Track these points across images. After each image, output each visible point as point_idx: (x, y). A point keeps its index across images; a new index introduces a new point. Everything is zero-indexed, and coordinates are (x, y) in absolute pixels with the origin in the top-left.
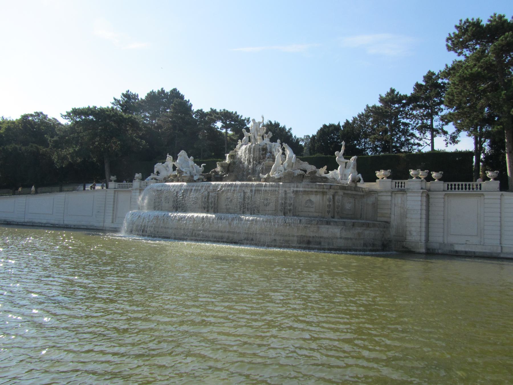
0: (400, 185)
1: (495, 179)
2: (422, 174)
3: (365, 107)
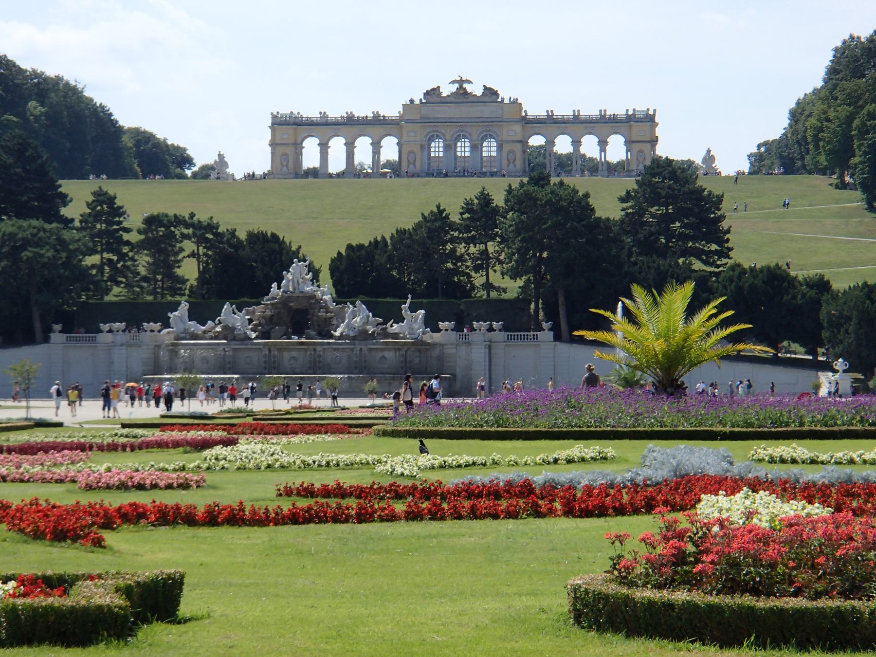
1: (550, 330)
2: (485, 325)
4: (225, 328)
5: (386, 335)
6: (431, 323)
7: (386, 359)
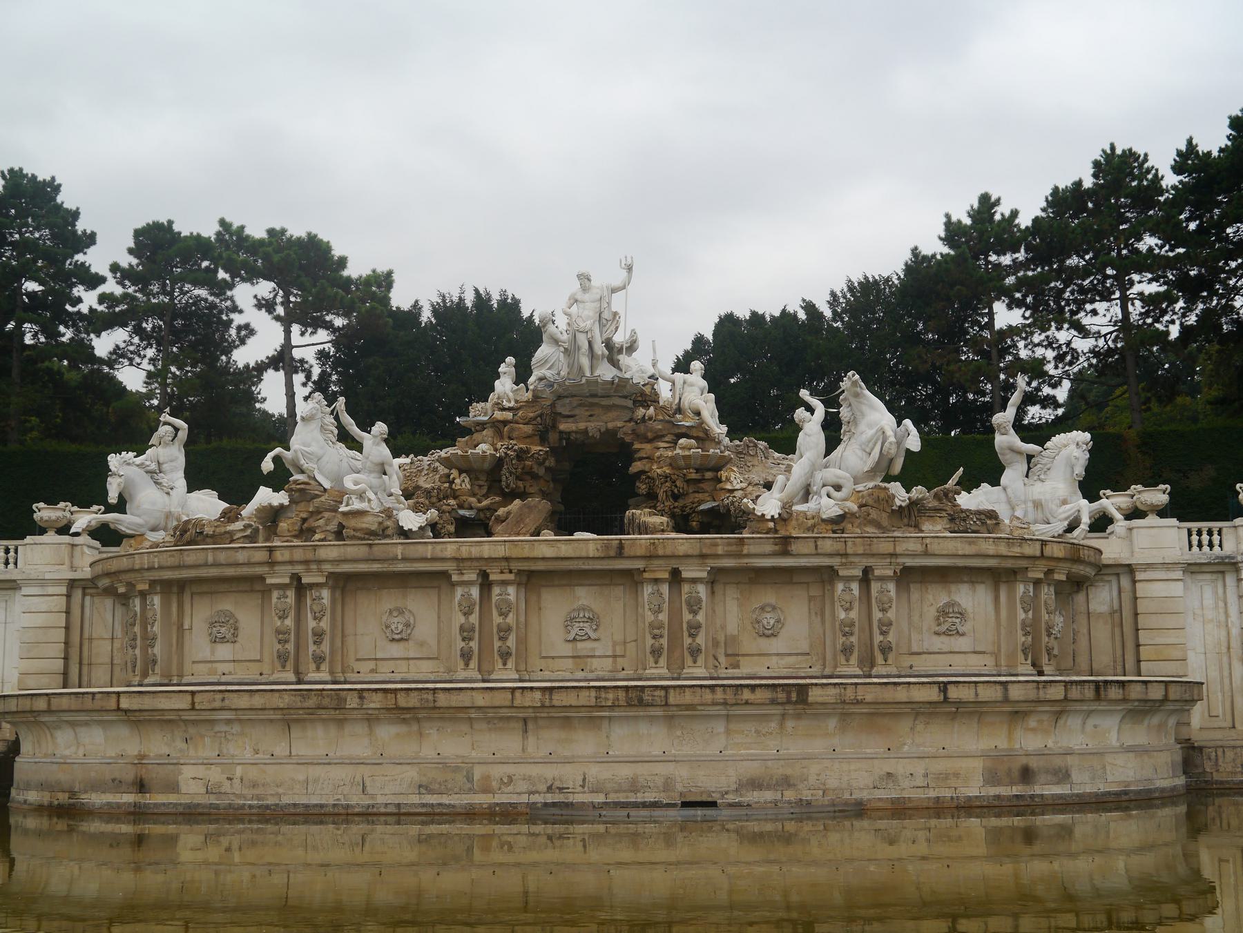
0: (1205, 538)
3: (907, 256)
4: (302, 494)
5: (959, 520)
6: (1089, 488)
7: (962, 615)
